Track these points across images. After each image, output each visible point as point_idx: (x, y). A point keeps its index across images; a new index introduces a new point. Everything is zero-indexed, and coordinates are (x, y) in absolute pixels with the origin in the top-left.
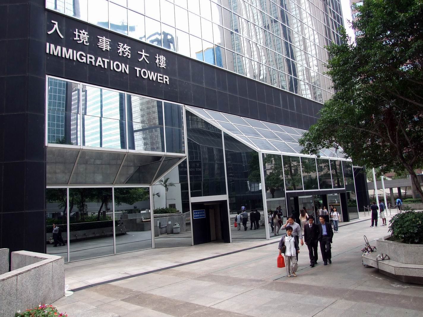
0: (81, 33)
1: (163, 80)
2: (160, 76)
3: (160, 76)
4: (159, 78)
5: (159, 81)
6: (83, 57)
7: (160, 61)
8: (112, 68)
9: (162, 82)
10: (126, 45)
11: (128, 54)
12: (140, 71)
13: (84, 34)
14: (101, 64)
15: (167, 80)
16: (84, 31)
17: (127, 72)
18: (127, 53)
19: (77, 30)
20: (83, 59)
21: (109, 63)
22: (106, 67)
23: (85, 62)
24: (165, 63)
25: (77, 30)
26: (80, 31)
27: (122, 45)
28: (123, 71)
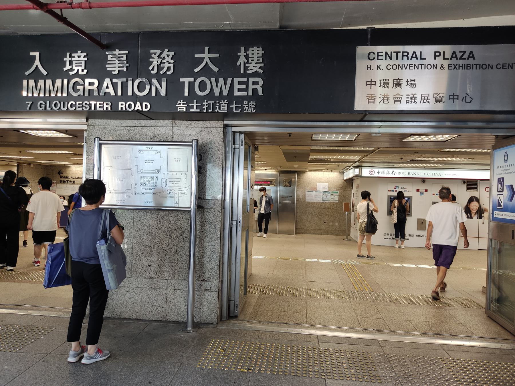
0: (74, 57)
1: (246, 90)
2: (239, 83)
3: (239, 83)
4: (236, 86)
5: (236, 93)
6: (78, 87)
7: (250, 59)
8: (130, 94)
9: (244, 94)
10: (166, 50)
11: (170, 65)
12: (191, 85)
13: (79, 57)
14: (111, 90)
15: (259, 87)
16: (79, 53)
17: (163, 93)
18: (166, 65)
19: (68, 54)
20: (79, 90)
21: (124, 86)
22: (119, 93)
23: (82, 94)
24: (261, 61)
25: (68, 54)
26: (73, 55)
27: (157, 55)
28: (153, 94)
